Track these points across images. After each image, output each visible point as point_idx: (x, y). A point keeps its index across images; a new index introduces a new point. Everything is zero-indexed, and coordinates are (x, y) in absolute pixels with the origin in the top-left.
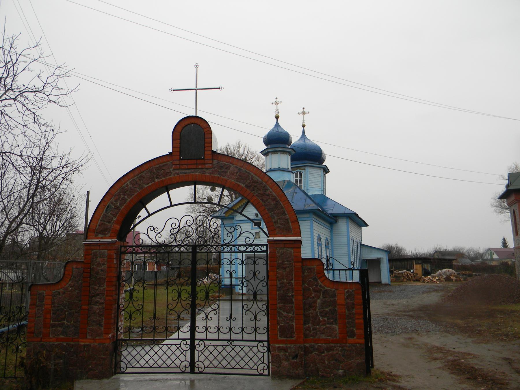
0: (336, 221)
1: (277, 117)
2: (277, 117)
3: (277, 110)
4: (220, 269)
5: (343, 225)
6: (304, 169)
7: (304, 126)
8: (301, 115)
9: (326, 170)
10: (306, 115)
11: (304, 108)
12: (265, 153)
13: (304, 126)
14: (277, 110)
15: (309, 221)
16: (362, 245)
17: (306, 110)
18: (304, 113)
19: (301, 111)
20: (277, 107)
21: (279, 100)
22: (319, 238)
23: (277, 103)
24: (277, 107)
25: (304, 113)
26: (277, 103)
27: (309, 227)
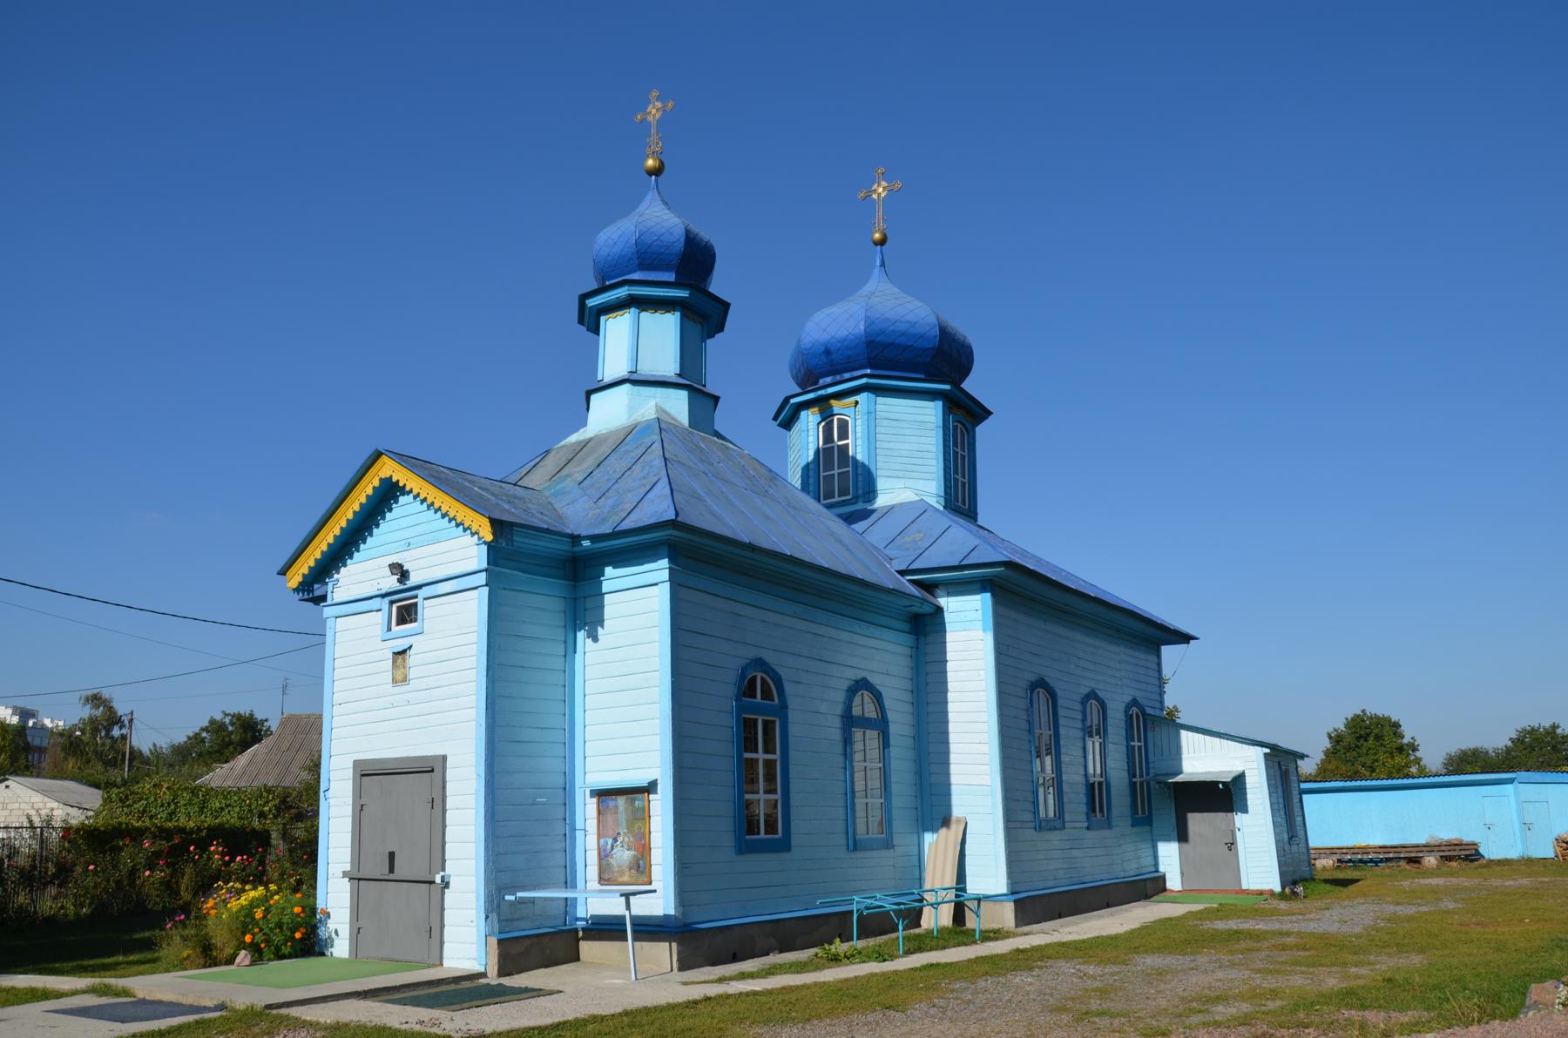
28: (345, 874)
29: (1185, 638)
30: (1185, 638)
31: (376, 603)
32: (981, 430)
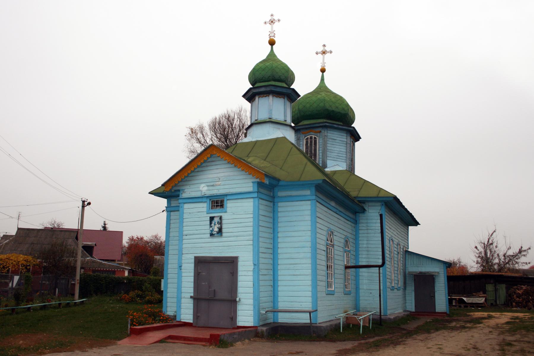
0: (364, 211)
1: (272, 43)
2: (272, 43)
3: (272, 32)
4: (163, 280)
5: (373, 214)
6: (320, 132)
7: (323, 71)
8: (320, 55)
9: (355, 137)
10: (328, 55)
11: (324, 46)
12: (250, 96)
13: (323, 71)
14: (272, 32)
15: (309, 202)
16: (407, 253)
17: (327, 49)
18: (324, 53)
19: (321, 49)
20: (272, 28)
21: (276, 17)
22: (331, 233)
23: (272, 22)
24: (272, 28)
25: (324, 53)
26: (272, 22)
27: (309, 212)
28: (191, 297)
29: (416, 223)
30: (416, 223)
31: (204, 200)
32: (357, 144)
